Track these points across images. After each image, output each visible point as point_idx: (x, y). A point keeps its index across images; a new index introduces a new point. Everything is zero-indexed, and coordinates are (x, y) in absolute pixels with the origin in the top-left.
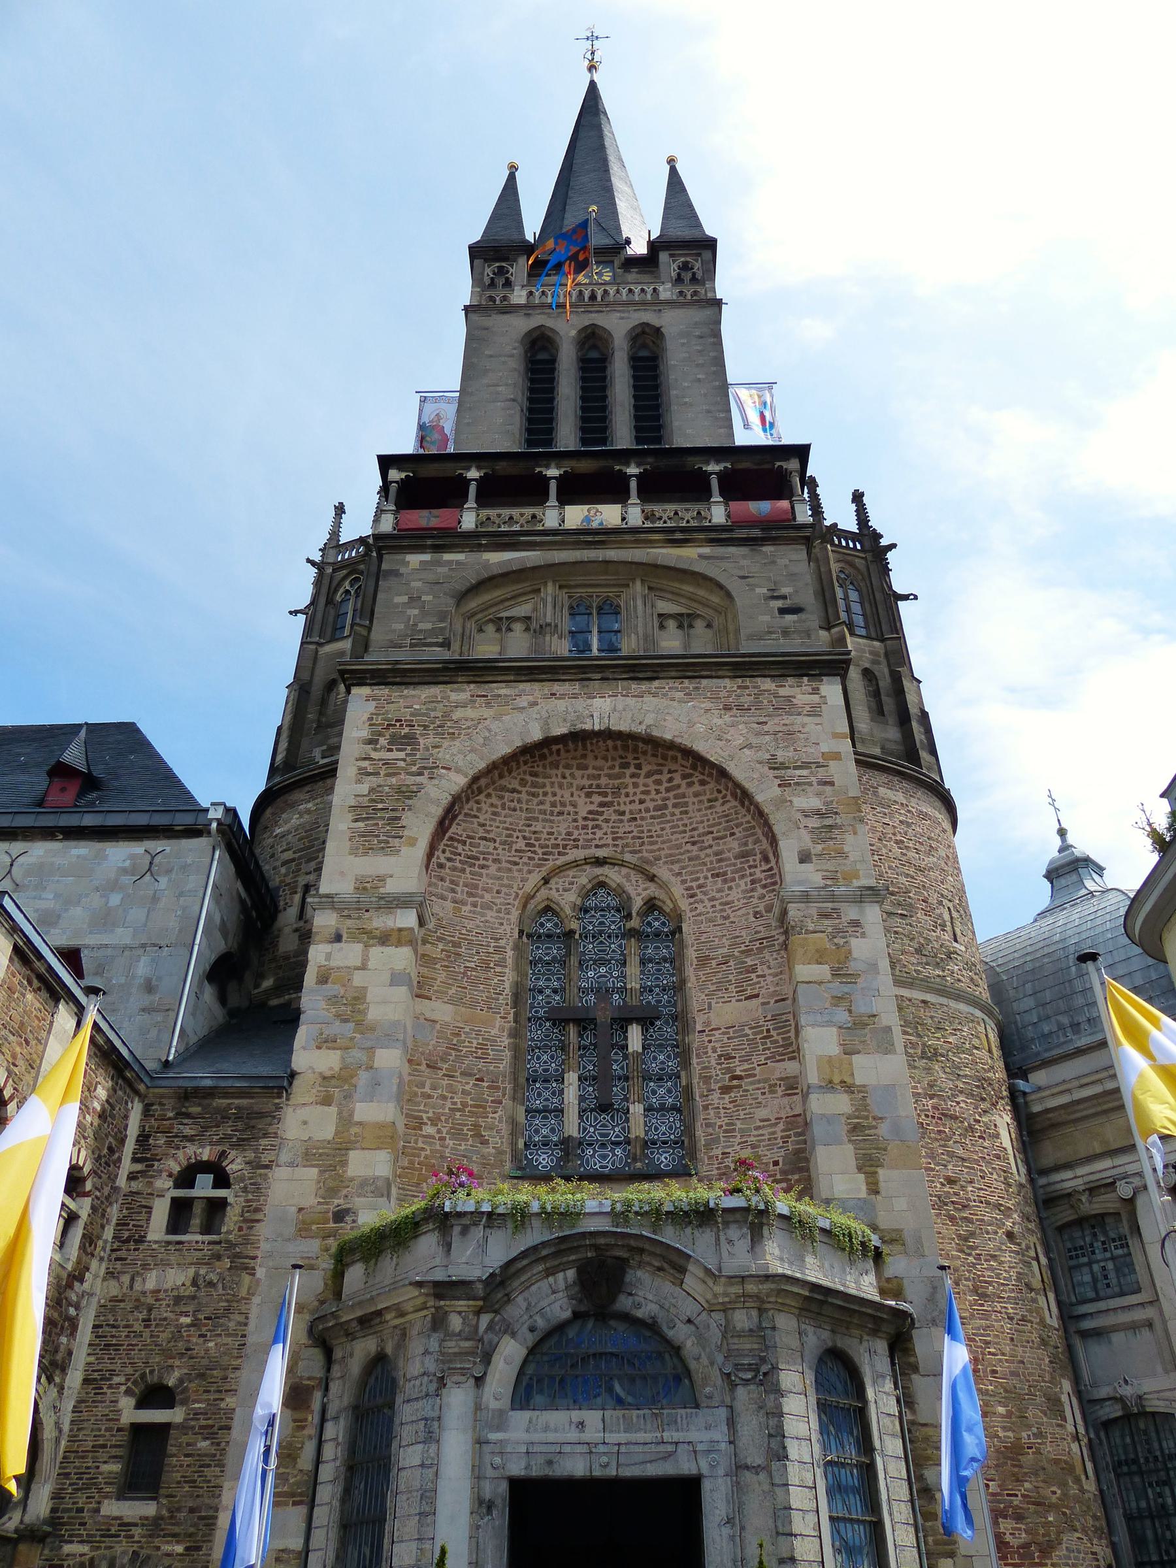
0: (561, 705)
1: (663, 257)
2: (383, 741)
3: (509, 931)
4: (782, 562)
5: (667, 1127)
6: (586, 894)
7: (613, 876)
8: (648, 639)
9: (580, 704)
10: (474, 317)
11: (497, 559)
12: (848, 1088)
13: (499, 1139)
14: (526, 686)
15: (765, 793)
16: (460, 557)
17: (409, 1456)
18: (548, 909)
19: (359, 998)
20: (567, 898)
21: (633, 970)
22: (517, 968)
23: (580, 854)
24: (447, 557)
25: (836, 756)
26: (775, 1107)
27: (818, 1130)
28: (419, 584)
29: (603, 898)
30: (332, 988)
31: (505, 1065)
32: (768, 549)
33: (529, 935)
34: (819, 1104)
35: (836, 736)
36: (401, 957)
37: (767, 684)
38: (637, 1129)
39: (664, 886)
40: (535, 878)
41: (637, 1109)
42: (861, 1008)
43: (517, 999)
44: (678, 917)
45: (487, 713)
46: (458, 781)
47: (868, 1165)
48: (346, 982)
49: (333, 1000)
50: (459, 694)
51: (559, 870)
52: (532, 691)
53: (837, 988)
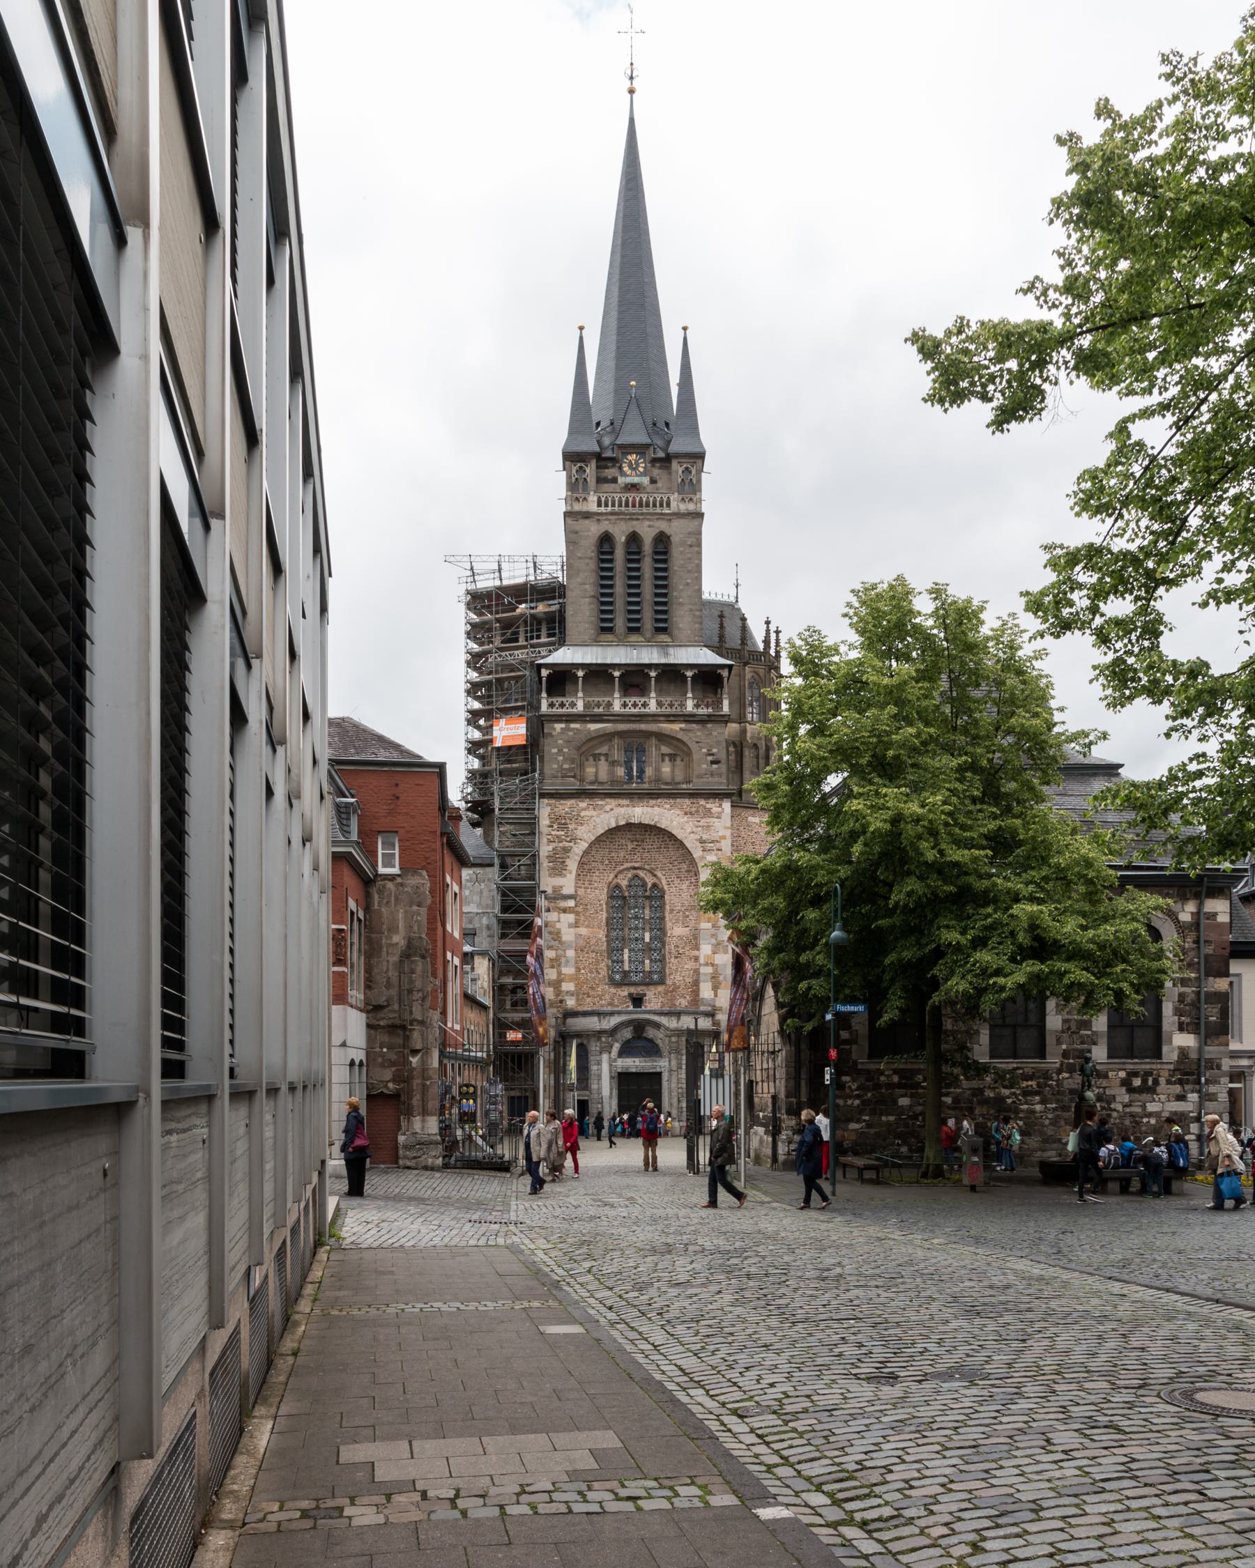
0: (622, 810)
1: (675, 464)
2: (555, 826)
3: (604, 897)
4: (715, 733)
5: (656, 967)
6: (631, 880)
7: (641, 873)
8: (658, 770)
9: (630, 810)
10: (569, 521)
11: (593, 727)
12: (712, 965)
13: (604, 972)
14: (608, 800)
15: (697, 853)
16: (576, 726)
17: (594, 1068)
18: (618, 886)
19: (558, 933)
20: (624, 883)
21: (647, 912)
22: (607, 912)
23: (627, 865)
24: (573, 726)
25: (724, 837)
26: (690, 965)
27: (702, 978)
28: (560, 742)
29: (637, 882)
30: (549, 929)
31: (604, 947)
32: (709, 726)
33: (611, 897)
34: (704, 970)
35: (726, 828)
36: (571, 918)
37: (702, 802)
38: (647, 969)
39: (659, 879)
40: (612, 876)
41: (647, 962)
42: (720, 939)
43: (607, 924)
44: (663, 892)
45: (594, 813)
46: (586, 845)
47: (715, 988)
48: (554, 927)
49: (550, 933)
50: (583, 805)
51: (620, 872)
52: (611, 803)
53: (713, 931)
